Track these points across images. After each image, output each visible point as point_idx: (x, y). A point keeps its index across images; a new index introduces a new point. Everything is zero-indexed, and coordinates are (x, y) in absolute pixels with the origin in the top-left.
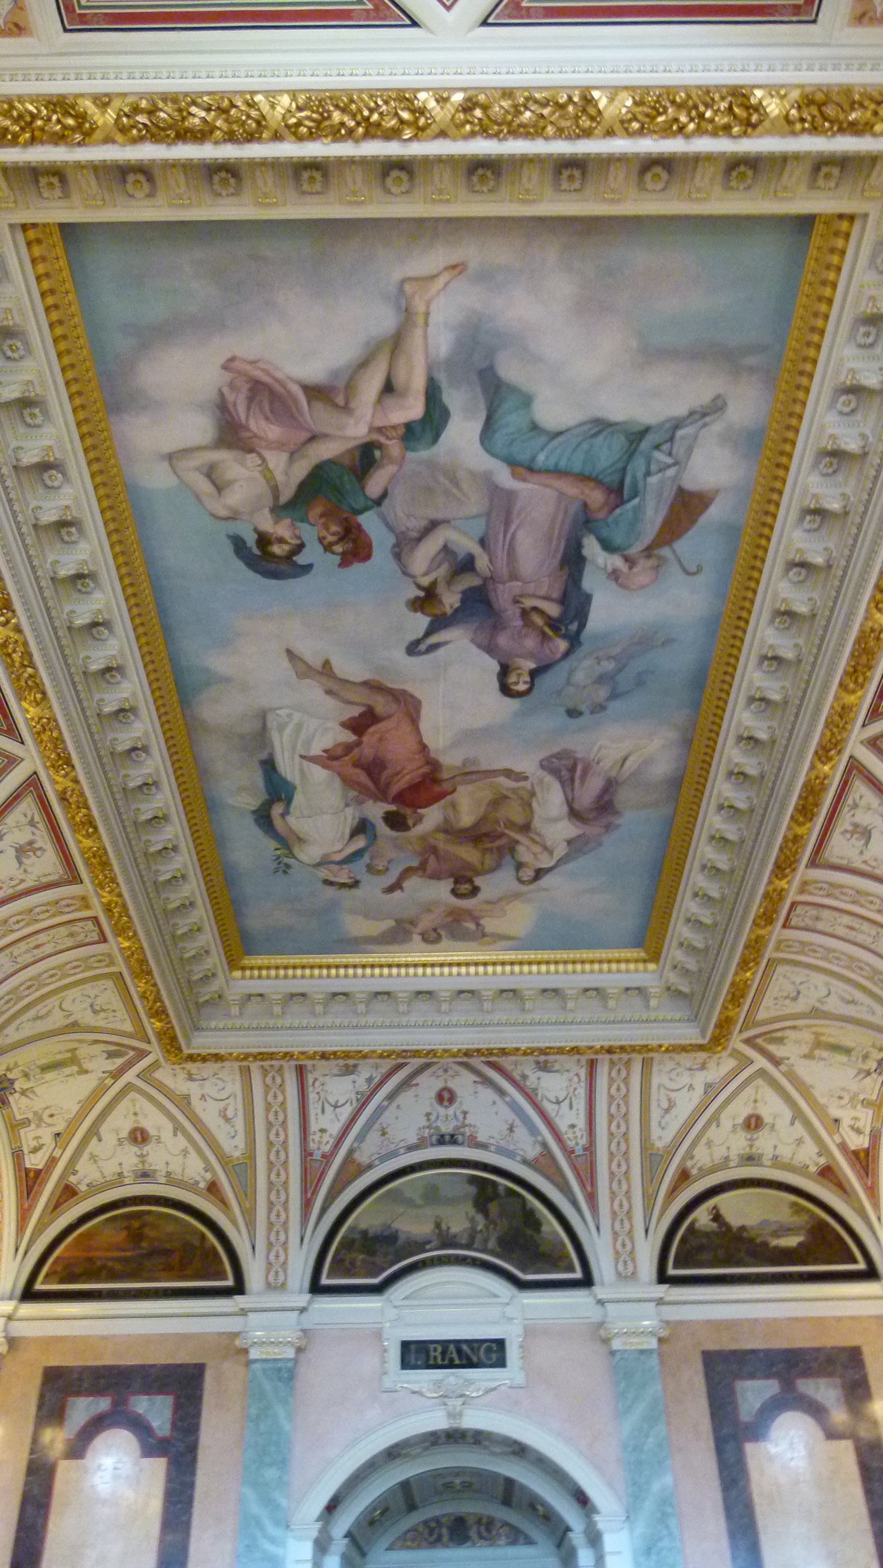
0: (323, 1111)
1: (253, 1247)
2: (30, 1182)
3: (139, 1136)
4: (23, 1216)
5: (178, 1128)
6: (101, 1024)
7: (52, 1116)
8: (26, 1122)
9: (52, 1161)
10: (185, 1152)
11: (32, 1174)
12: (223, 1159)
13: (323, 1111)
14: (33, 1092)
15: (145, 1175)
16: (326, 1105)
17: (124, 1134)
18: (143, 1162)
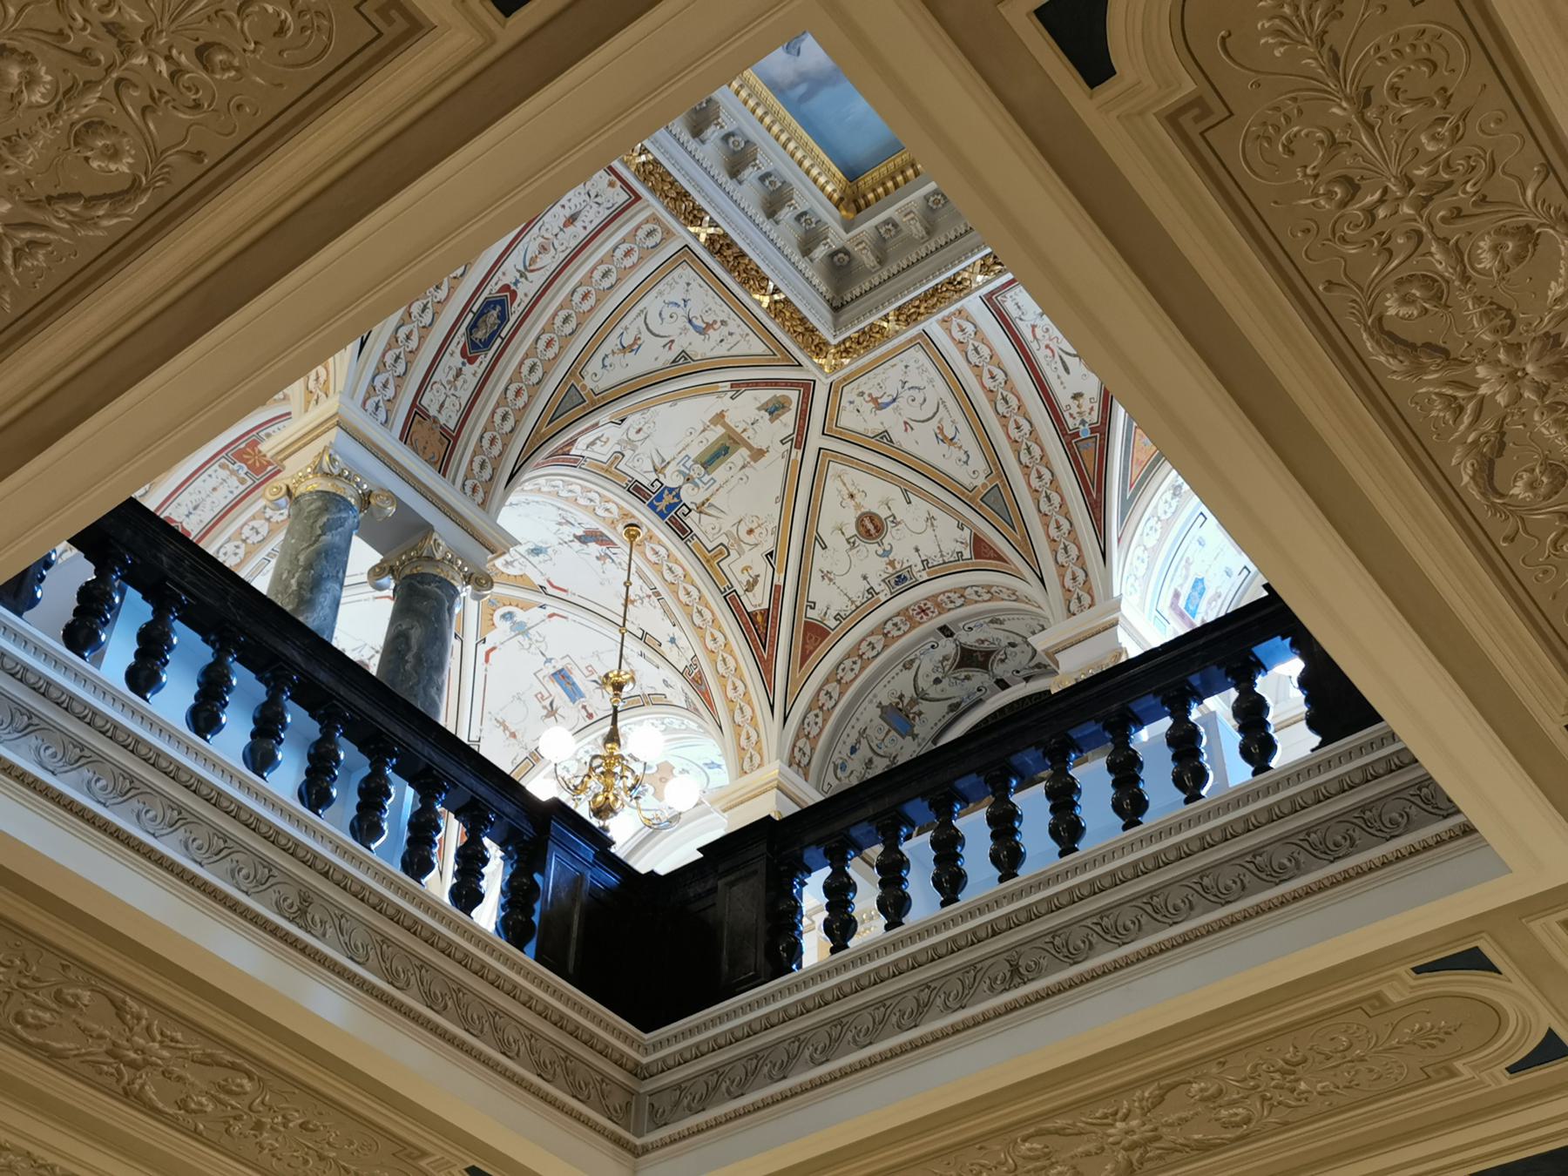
0: (1067, 370)
1: (1042, 580)
2: (759, 629)
3: (871, 527)
4: (766, 668)
5: (907, 490)
6: (722, 350)
7: (750, 532)
8: (723, 551)
9: (777, 592)
10: (931, 519)
11: (759, 618)
12: (963, 494)
13: (1067, 370)
14: (711, 505)
15: (901, 581)
16: (1065, 357)
17: (851, 530)
18: (891, 563)
